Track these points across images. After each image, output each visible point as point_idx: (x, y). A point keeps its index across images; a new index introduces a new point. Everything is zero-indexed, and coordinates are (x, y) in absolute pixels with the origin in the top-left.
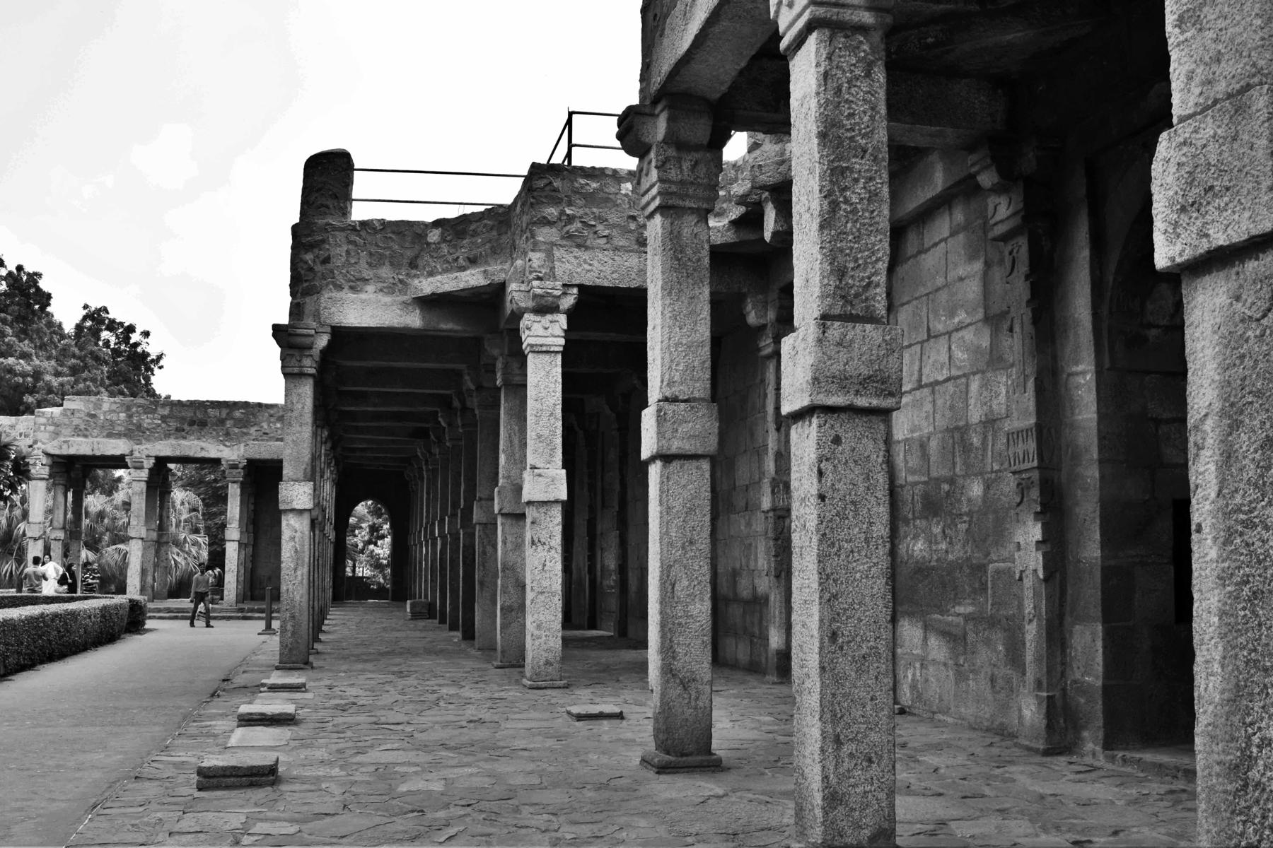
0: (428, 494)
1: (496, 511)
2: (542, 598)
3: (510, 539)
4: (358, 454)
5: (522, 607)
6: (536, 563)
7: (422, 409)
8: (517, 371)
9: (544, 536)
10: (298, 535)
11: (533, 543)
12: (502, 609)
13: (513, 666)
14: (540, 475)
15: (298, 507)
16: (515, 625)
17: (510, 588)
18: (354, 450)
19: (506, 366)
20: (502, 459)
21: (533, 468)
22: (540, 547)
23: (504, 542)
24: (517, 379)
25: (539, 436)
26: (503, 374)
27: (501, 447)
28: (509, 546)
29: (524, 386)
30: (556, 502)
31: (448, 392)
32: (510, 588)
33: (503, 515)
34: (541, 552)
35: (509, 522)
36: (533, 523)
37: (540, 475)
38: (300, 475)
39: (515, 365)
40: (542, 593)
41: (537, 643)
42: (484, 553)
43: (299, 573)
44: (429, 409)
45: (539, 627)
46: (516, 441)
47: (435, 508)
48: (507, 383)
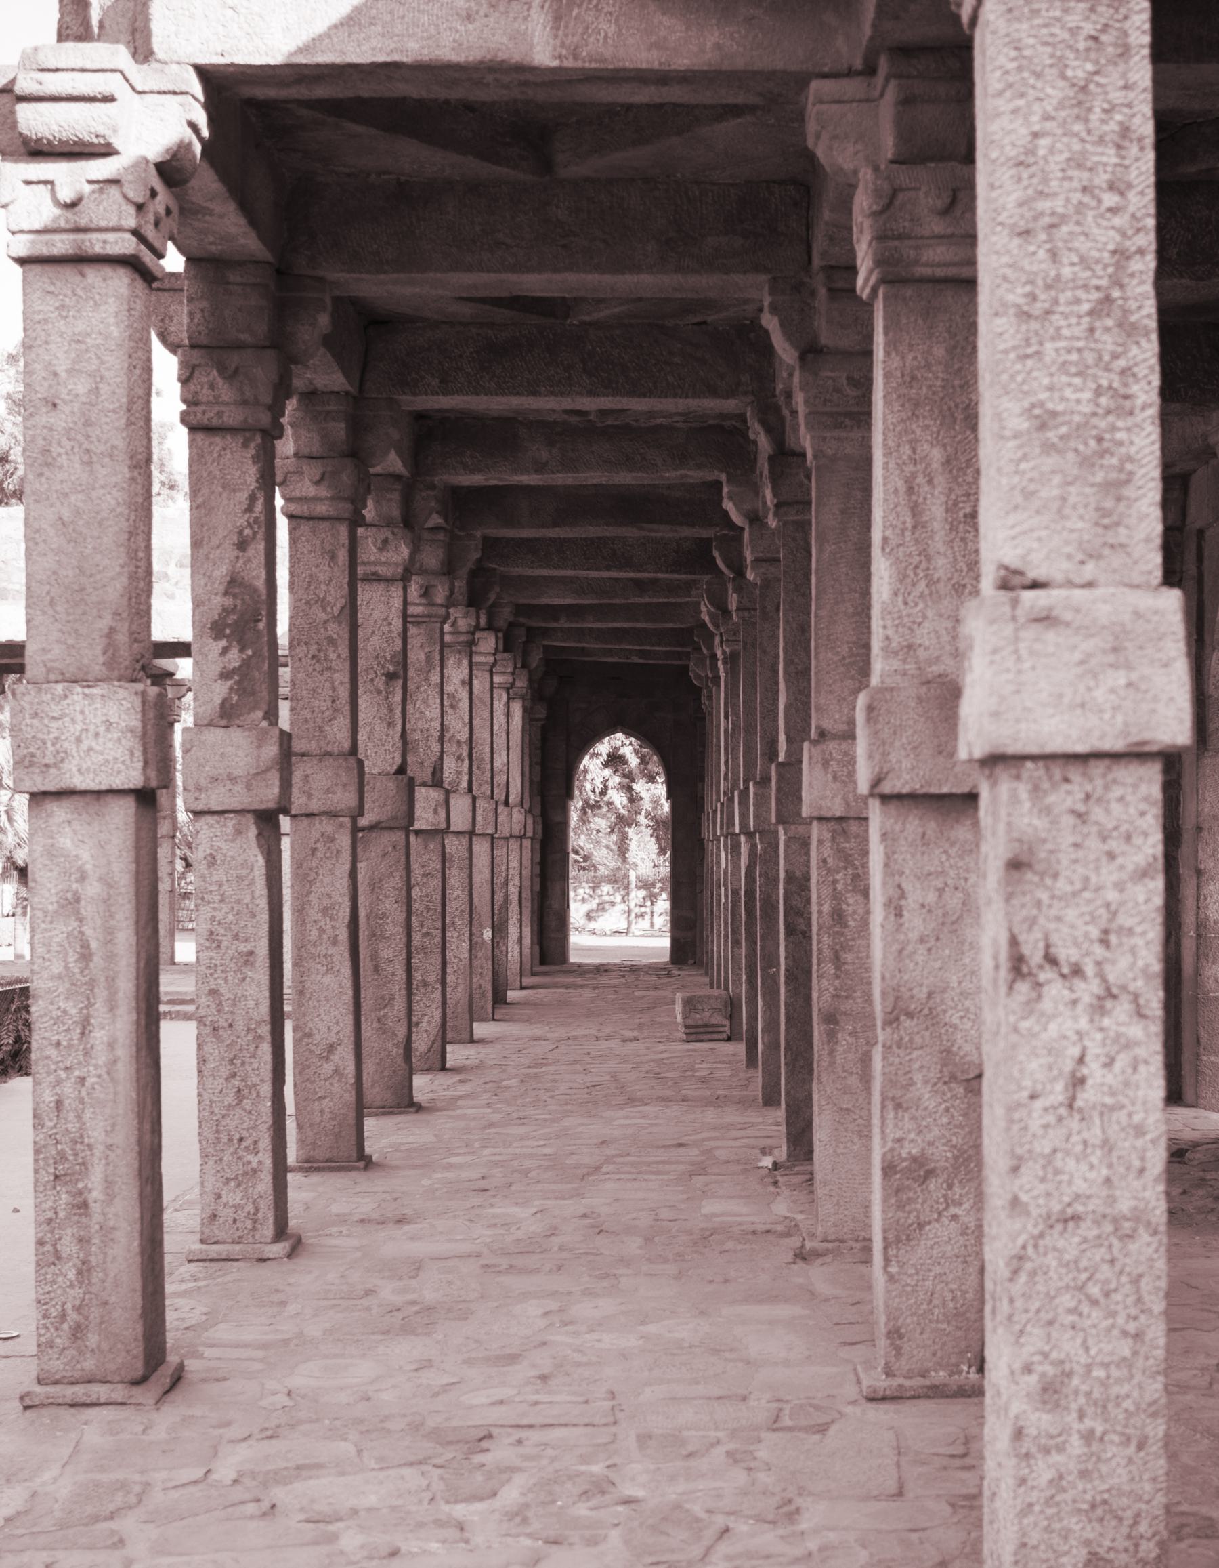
0: (726, 717)
1: (863, 787)
2: (1069, 1243)
3: (916, 894)
4: (564, 623)
5: (968, 1161)
6: (1035, 1068)
7: (672, 475)
8: (937, 226)
9: (1071, 932)
10: (92, 889)
11: (1018, 965)
12: (889, 1169)
13: (935, 1392)
14: (1046, 619)
15: (80, 783)
16: (943, 1232)
17: (922, 1091)
18: (553, 612)
19: (889, 203)
20: (882, 571)
21: (1013, 581)
22: (1055, 991)
23: (896, 909)
24: (935, 257)
25: (1044, 420)
26: (881, 237)
27: (876, 535)
28: (915, 924)
29: (966, 285)
30: (1136, 755)
31: (730, 405)
32: (922, 1091)
33: (885, 799)
34: (1062, 1017)
35: (913, 824)
36: (1016, 865)
37: (1046, 619)
38: (93, 656)
39: (925, 200)
40: (1070, 1219)
41: (1043, 1472)
42: (838, 916)
43: (99, 1036)
44: (695, 475)
45: (1051, 1393)
46: (936, 510)
47: (736, 758)
48: (895, 275)
